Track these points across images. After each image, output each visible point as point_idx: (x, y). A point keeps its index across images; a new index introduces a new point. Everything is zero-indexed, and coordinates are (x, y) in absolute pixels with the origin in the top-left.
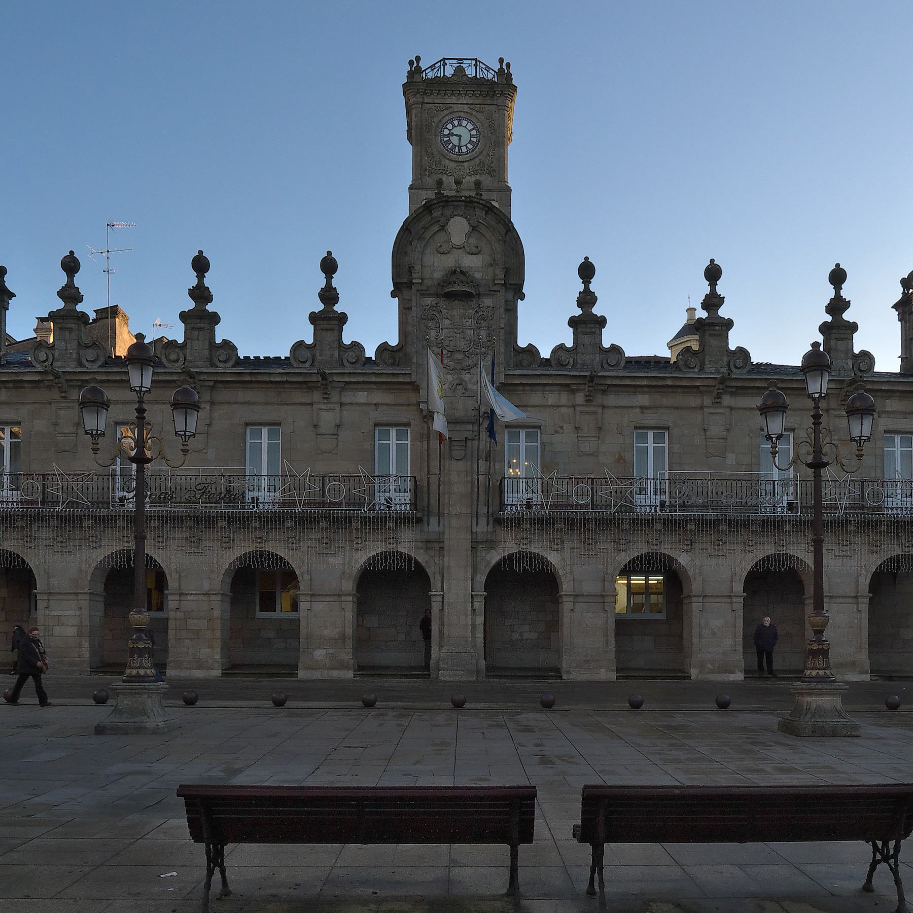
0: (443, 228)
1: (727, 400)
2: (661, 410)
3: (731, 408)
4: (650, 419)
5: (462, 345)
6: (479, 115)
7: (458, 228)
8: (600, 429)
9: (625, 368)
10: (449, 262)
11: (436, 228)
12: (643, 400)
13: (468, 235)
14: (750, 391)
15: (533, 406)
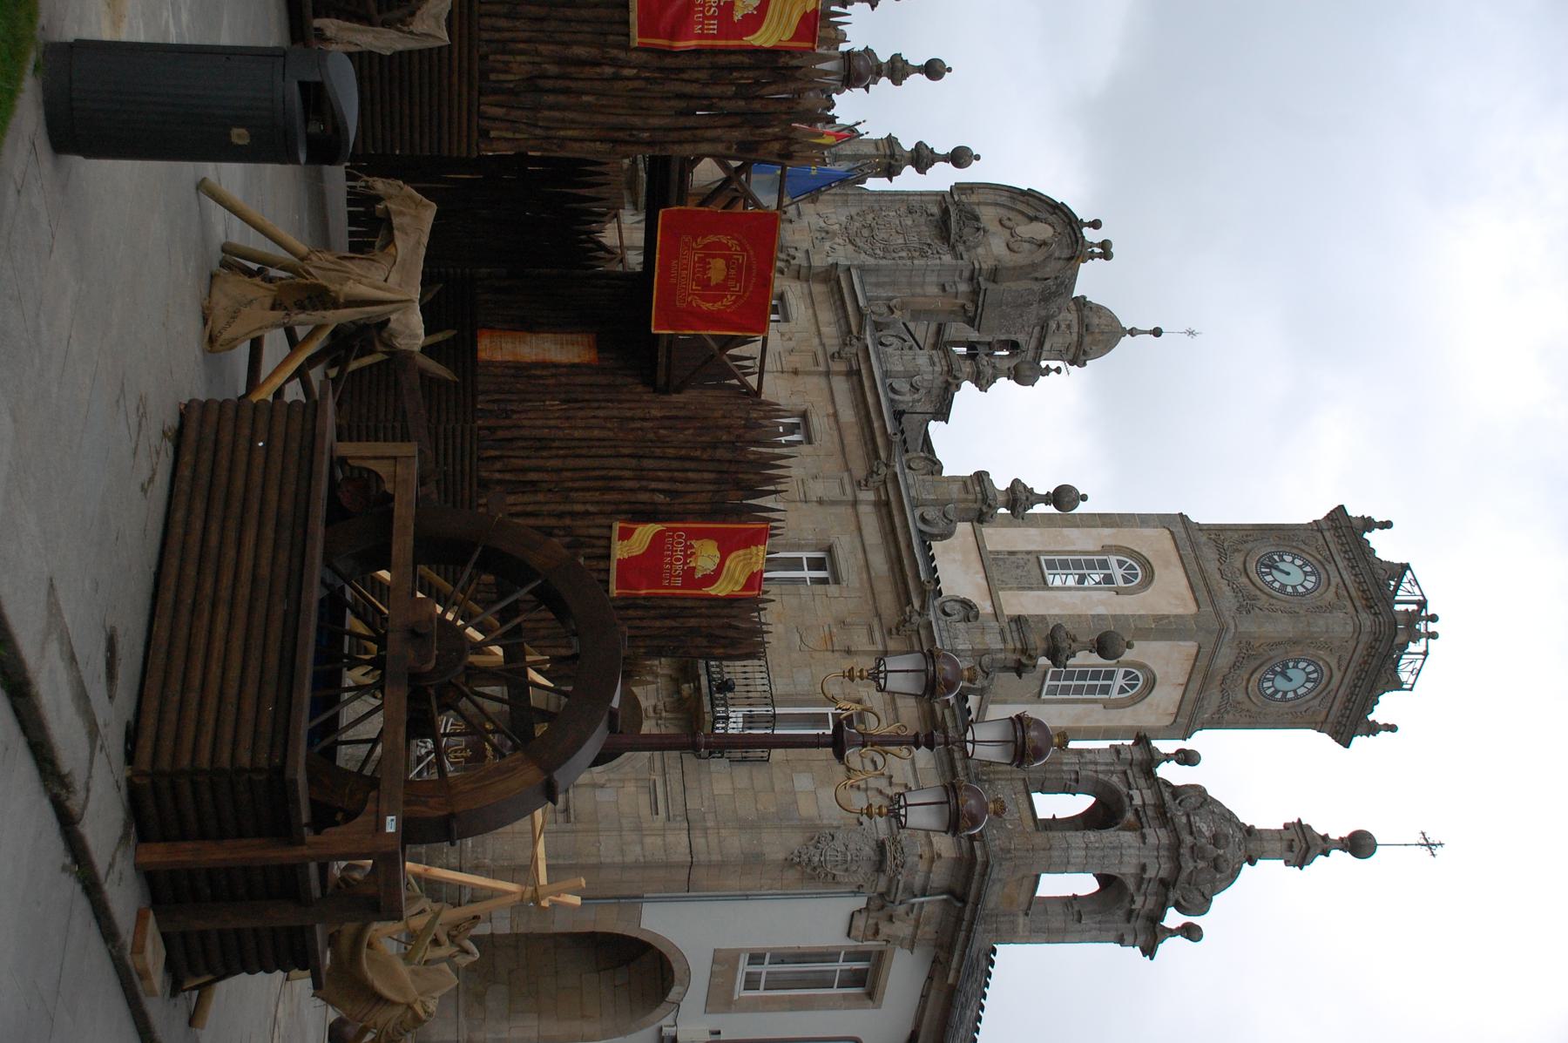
0: (1036, 219)
1: (869, 496)
2: (836, 433)
3: (855, 503)
4: (819, 423)
5: (882, 235)
6: (1330, 595)
7: (1042, 231)
8: (796, 372)
9: (892, 401)
10: (993, 227)
11: (1031, 213)
12: (848, 415)
13: (1031, 241)
14: (892, 545)
15: (815, 315)
